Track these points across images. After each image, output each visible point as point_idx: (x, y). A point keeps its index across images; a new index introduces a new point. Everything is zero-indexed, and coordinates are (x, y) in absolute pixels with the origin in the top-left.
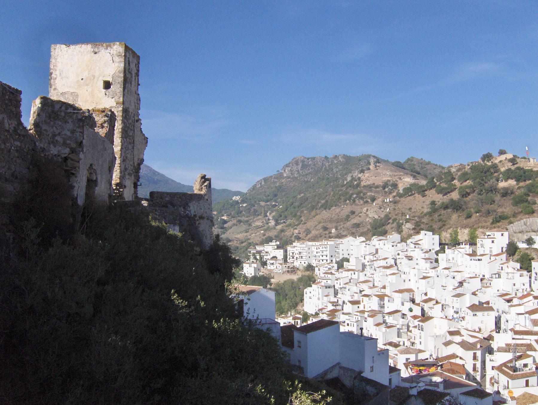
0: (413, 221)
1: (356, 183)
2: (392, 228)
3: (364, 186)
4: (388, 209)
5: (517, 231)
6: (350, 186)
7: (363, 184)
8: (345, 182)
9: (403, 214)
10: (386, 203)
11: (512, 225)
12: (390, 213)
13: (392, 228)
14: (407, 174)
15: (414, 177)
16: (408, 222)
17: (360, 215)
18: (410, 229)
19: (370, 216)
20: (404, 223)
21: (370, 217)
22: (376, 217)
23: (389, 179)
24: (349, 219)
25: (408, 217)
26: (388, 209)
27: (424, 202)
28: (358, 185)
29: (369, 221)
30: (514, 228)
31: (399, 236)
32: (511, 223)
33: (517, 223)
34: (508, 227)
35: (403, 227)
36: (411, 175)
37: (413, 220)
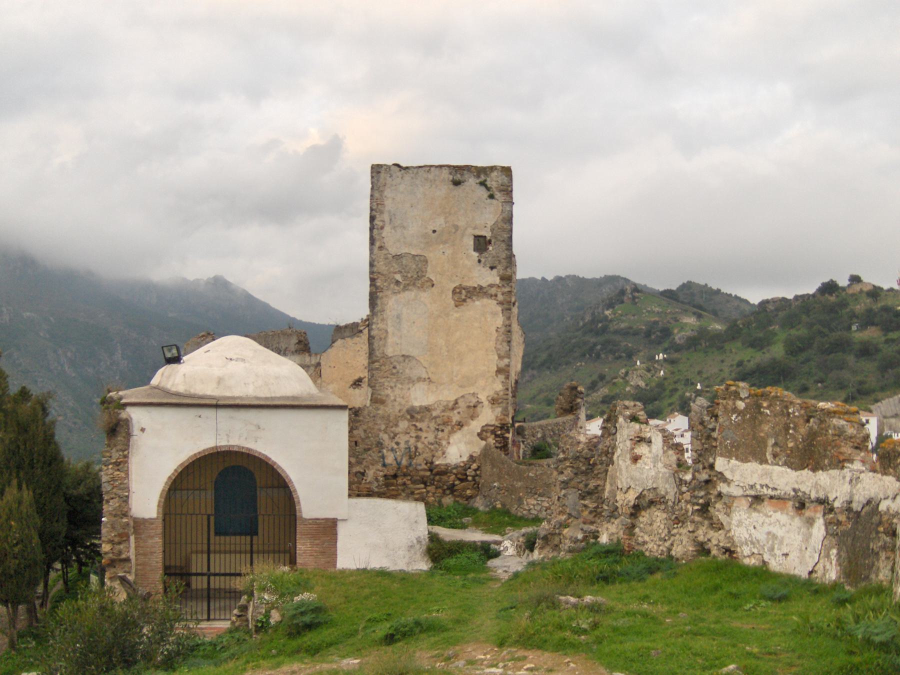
0: (708, 395)
1: (600, 325)
2: (670, 405)
3: (616, 332)
4: (662, 373)
5: (888, 415)
6: (591, 331)
7: (613, 327)
8: (581, 324)
9: (690, 383)
10: (658, 361)
11: (879, 404)
12: (665, 379)
13: (670, 405)
14: (686, 311)
15: (699, 316)
16: (700, 396)
17: (614, 381)
18: (703, 407)
19: (632, 383)
20: (693, 396)
21: (631, 385)
22: (642, 384)
23: (657, 319)
24: (596, 388)
25: (699, 387)
26: (662, 373)
27: (722, 361)
28: (604, 330)
29: (630, 391)
30: (882, 409)
31: (687, 418)
32: (877, 401)
33: (887, 400)
34: (872, 407)
35: (692, 404)
36: (694, 313)
37: (707, 392)
